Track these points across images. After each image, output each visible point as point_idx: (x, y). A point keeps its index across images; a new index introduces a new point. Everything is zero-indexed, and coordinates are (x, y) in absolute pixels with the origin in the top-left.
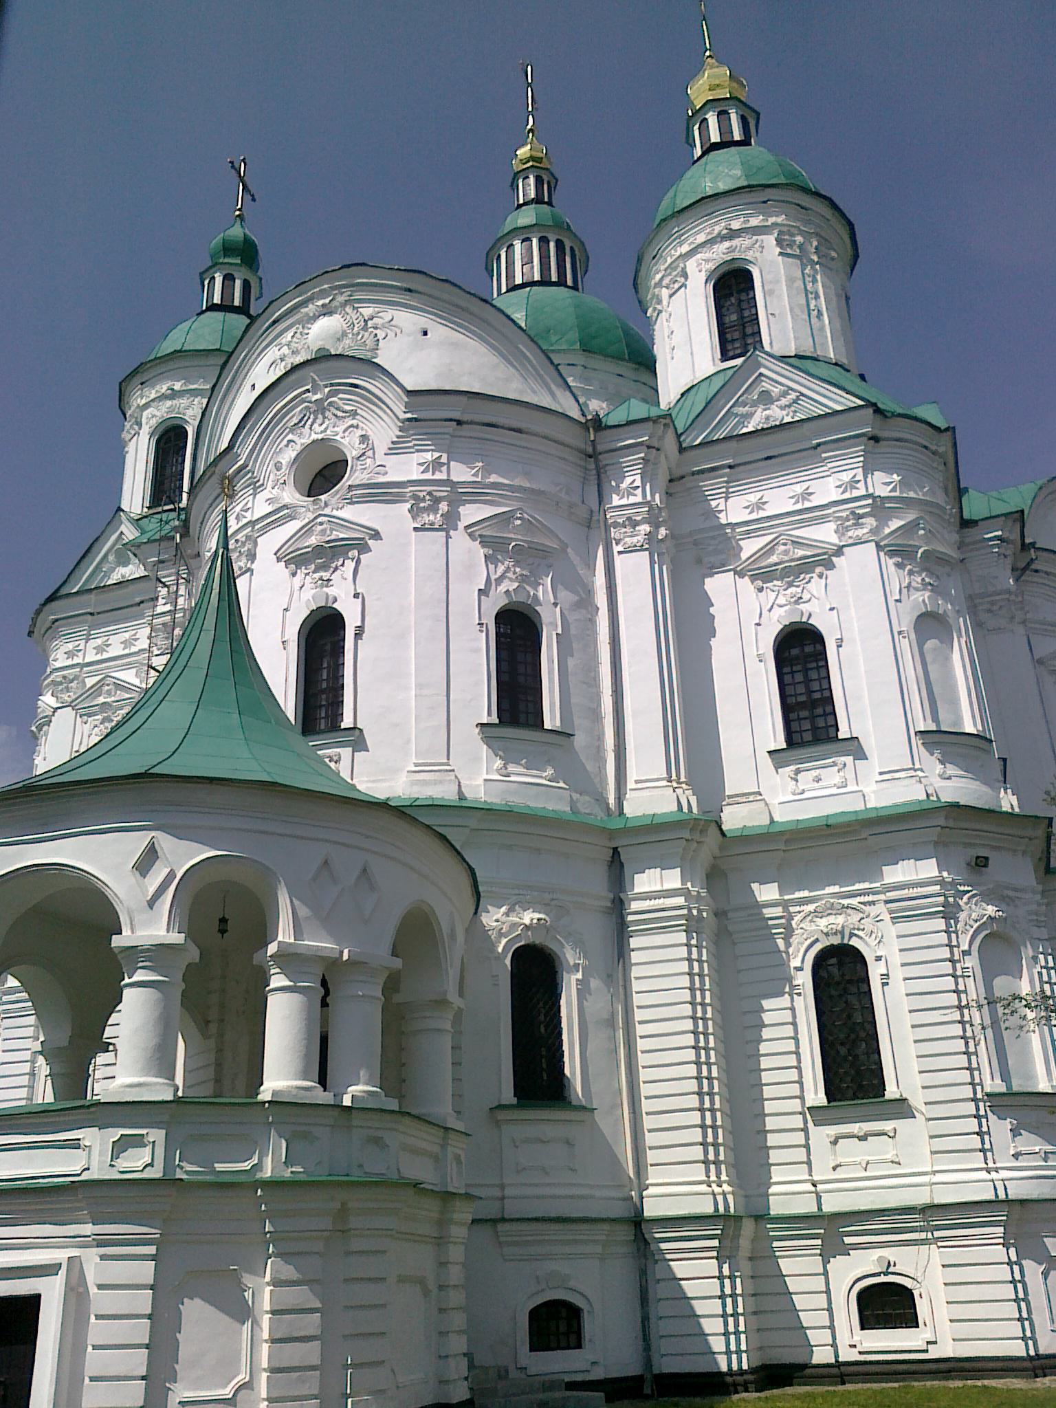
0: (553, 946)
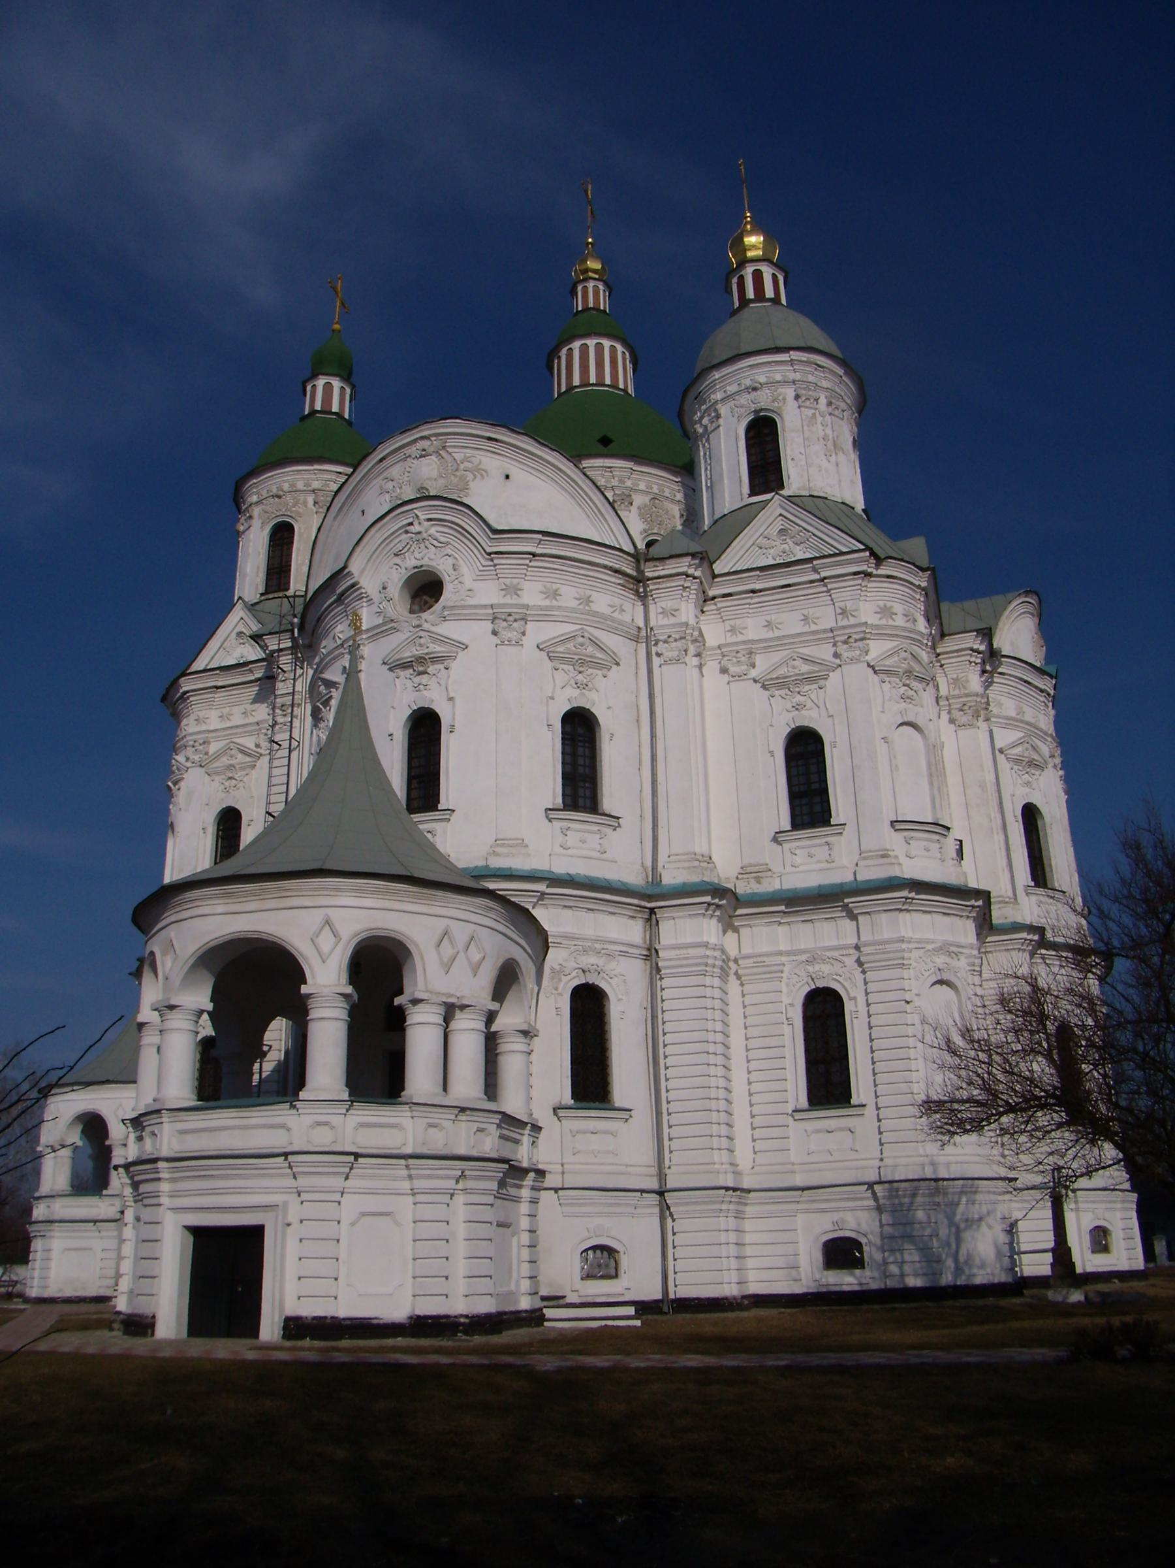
0: (603, 985)
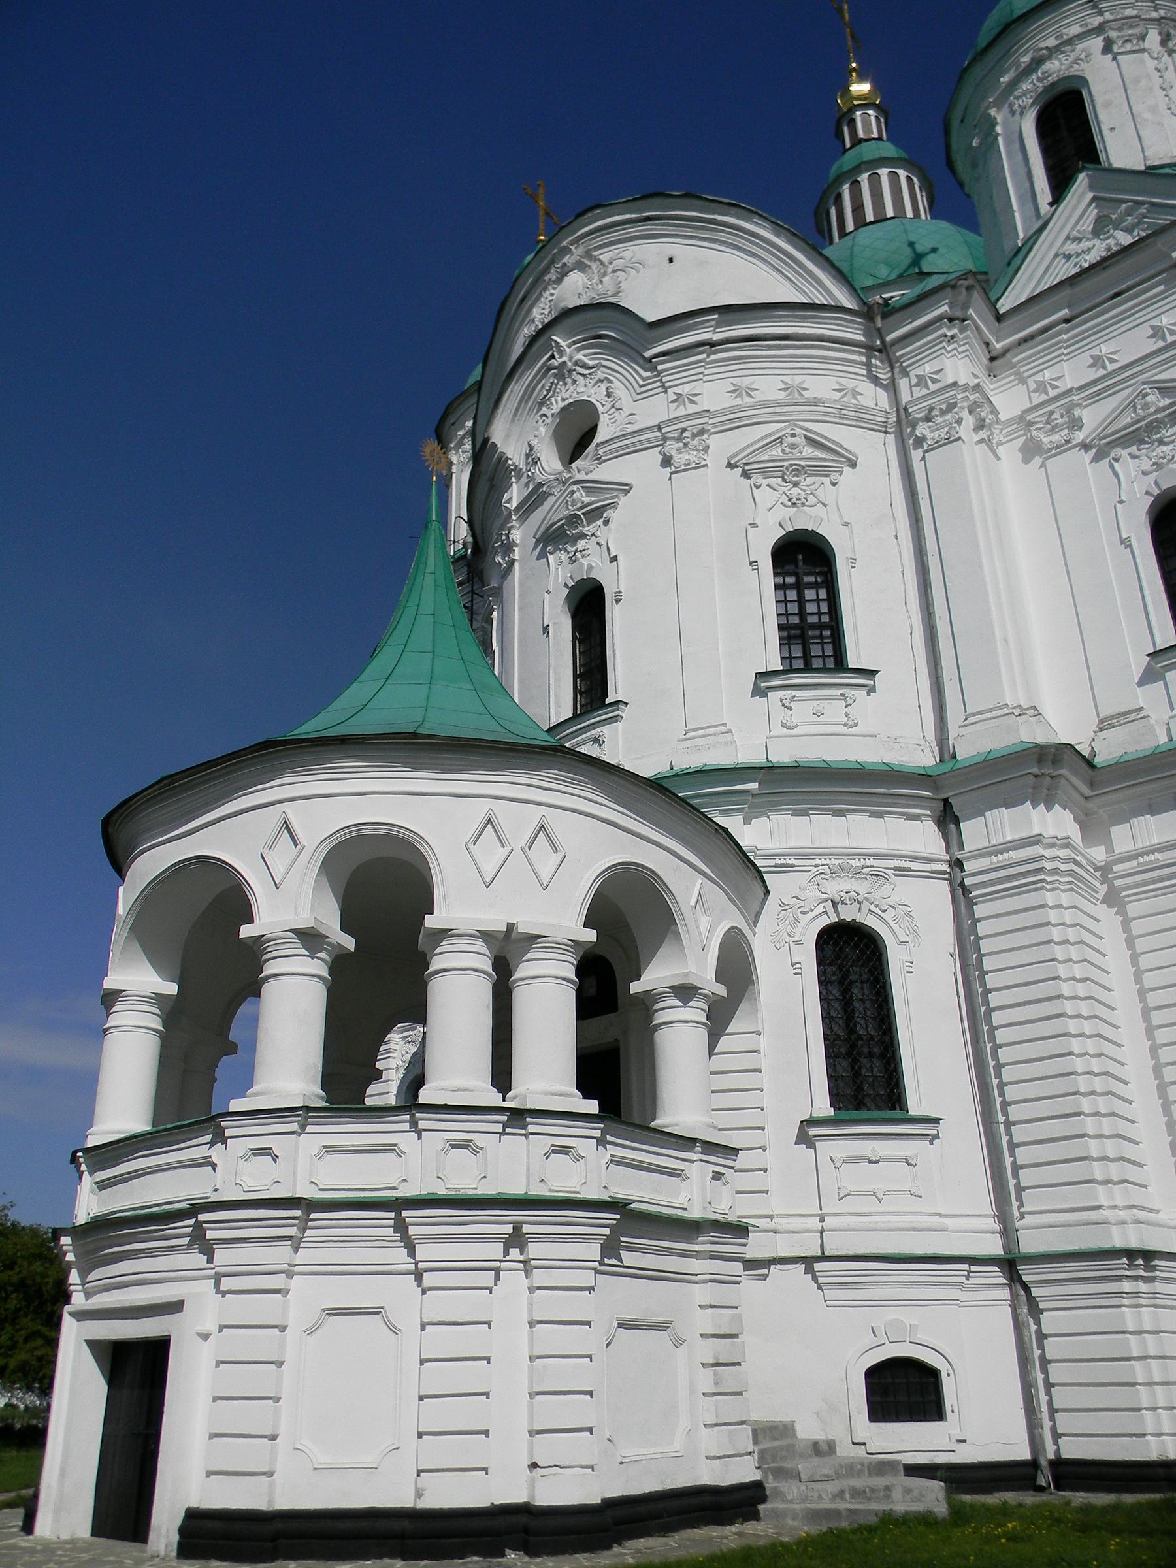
0: (871, 922)
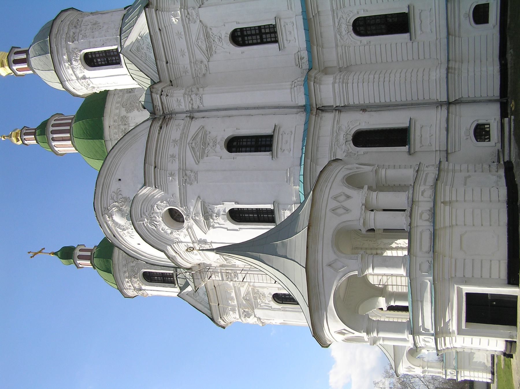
0: (353, 132)
